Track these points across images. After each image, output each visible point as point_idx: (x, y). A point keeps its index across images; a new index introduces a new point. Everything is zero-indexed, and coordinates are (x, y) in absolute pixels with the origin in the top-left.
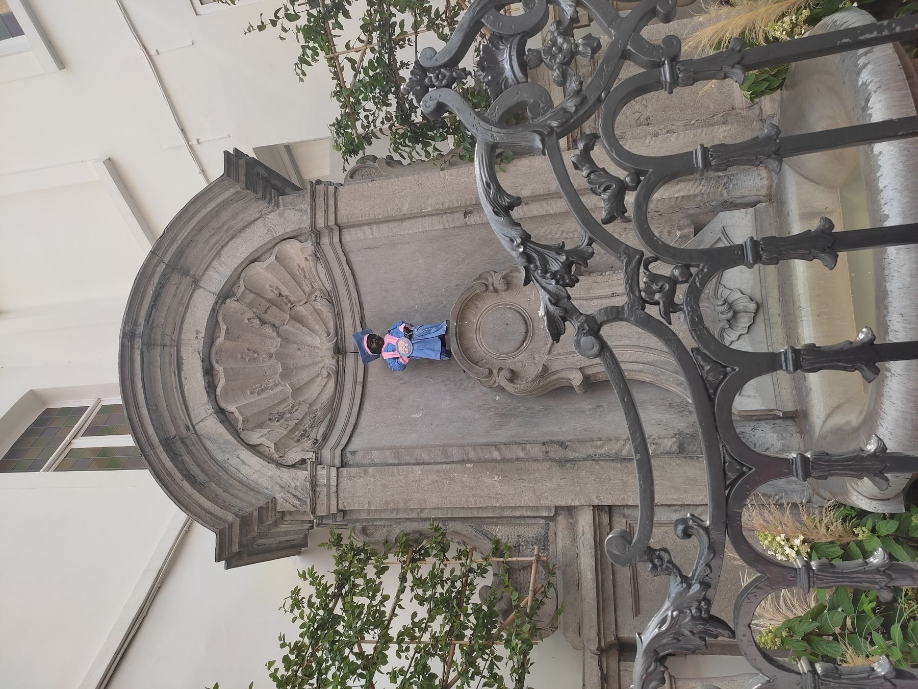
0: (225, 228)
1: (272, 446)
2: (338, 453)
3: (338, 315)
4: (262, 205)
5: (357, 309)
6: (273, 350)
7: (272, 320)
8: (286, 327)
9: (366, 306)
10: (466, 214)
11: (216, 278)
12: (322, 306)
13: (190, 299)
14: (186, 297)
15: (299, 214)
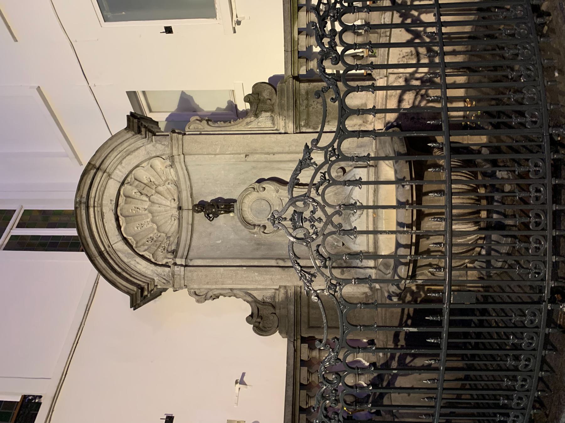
0: (125, 150)
1: (151, 255)
2: (184, 260)
3: (179, 192)
4: (145, 140)
5: (189, 190)
6: (146, 207)
7: (146, 193)
8: (153, 197)
9: (194, 189)
10: (246, 156)
11: (119, 174)
12: (171, 187)
13: (107, 184)
14: (105, 183)
15: (163, 147)
